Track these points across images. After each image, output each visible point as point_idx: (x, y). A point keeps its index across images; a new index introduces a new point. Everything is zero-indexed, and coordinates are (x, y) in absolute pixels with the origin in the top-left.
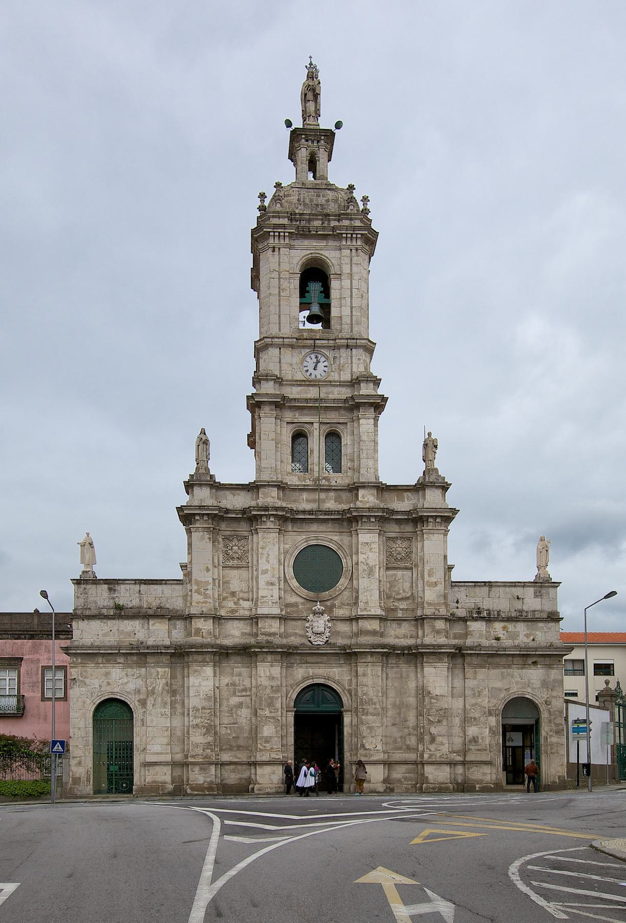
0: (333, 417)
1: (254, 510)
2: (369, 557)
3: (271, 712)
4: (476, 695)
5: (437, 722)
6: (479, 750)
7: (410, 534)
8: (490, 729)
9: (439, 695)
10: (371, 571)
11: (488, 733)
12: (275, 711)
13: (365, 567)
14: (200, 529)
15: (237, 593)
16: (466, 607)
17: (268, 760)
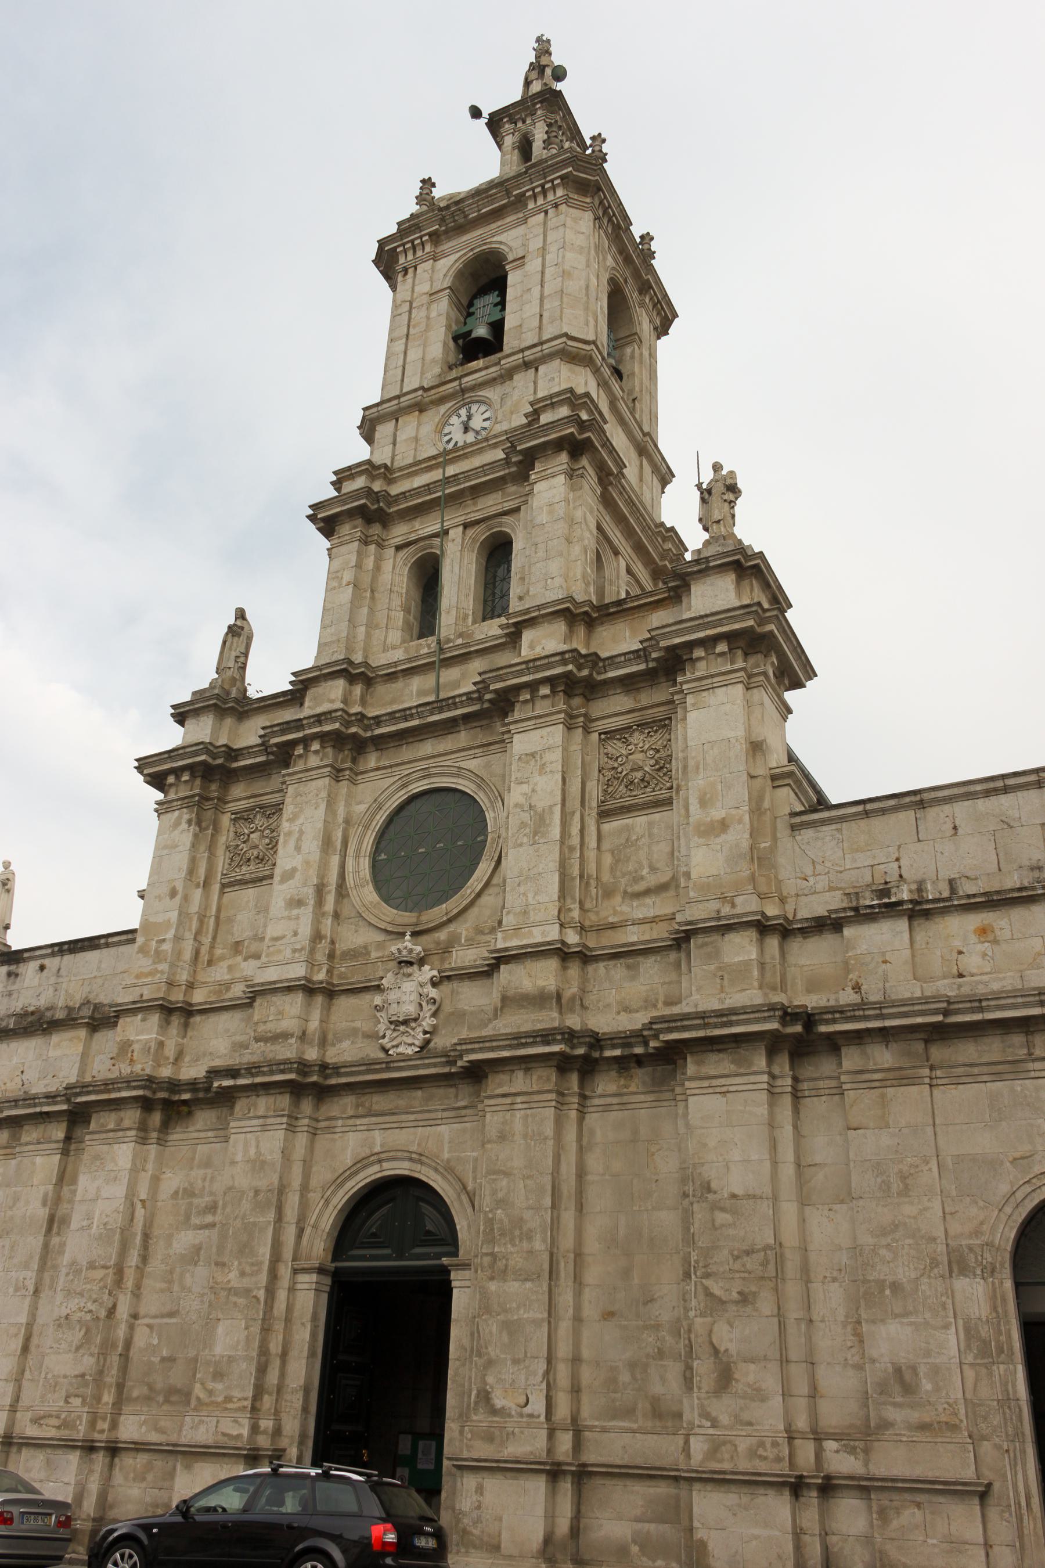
0: (490, 503)
1: (274, 734)
2: (538, 788)
3: (243, 1274)
4: (895, 1188)
5: (737, 1302)
6: (923, 1427)
7: (662, 709)
8: (970, 1332)
9: (739, 1192)
10: (541, 821)
11: (954, 1352)
12: (255, 1268)
13: (526, 817)
14: (175, 804)
15: (246, 944)
16: (843, 885)
17: (210, 1441)
